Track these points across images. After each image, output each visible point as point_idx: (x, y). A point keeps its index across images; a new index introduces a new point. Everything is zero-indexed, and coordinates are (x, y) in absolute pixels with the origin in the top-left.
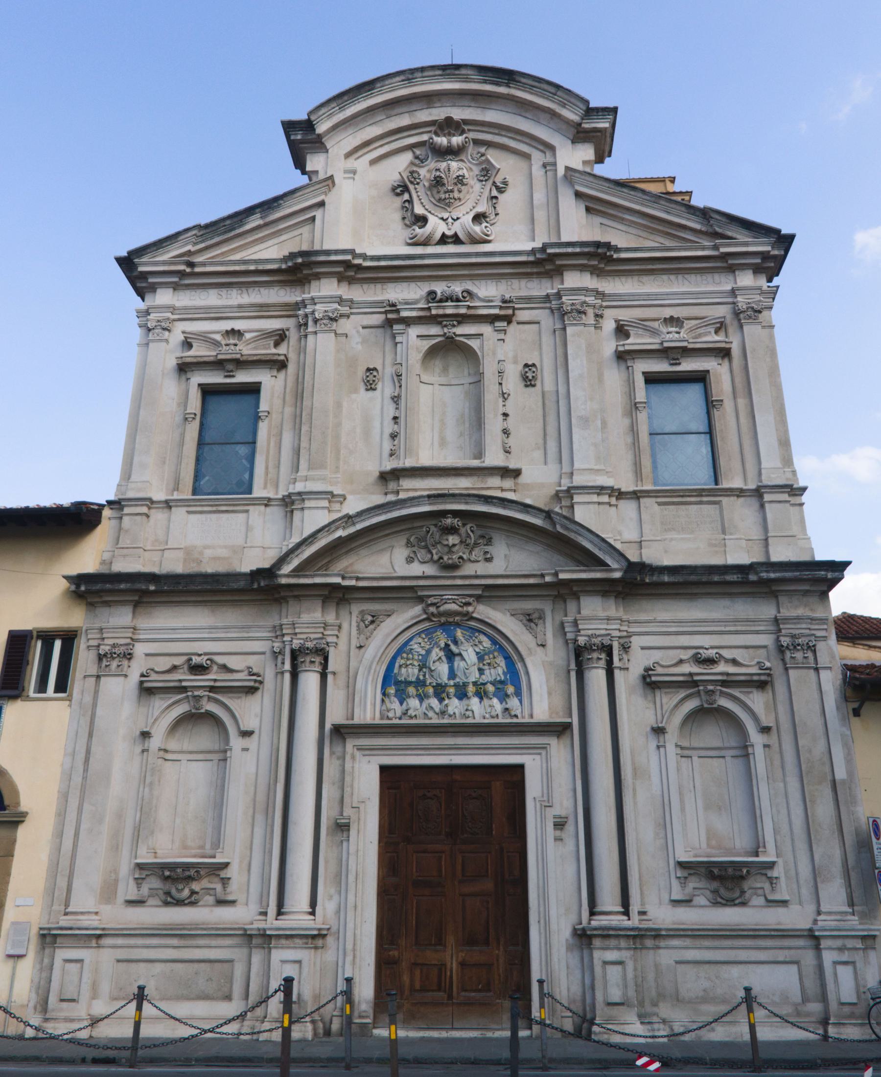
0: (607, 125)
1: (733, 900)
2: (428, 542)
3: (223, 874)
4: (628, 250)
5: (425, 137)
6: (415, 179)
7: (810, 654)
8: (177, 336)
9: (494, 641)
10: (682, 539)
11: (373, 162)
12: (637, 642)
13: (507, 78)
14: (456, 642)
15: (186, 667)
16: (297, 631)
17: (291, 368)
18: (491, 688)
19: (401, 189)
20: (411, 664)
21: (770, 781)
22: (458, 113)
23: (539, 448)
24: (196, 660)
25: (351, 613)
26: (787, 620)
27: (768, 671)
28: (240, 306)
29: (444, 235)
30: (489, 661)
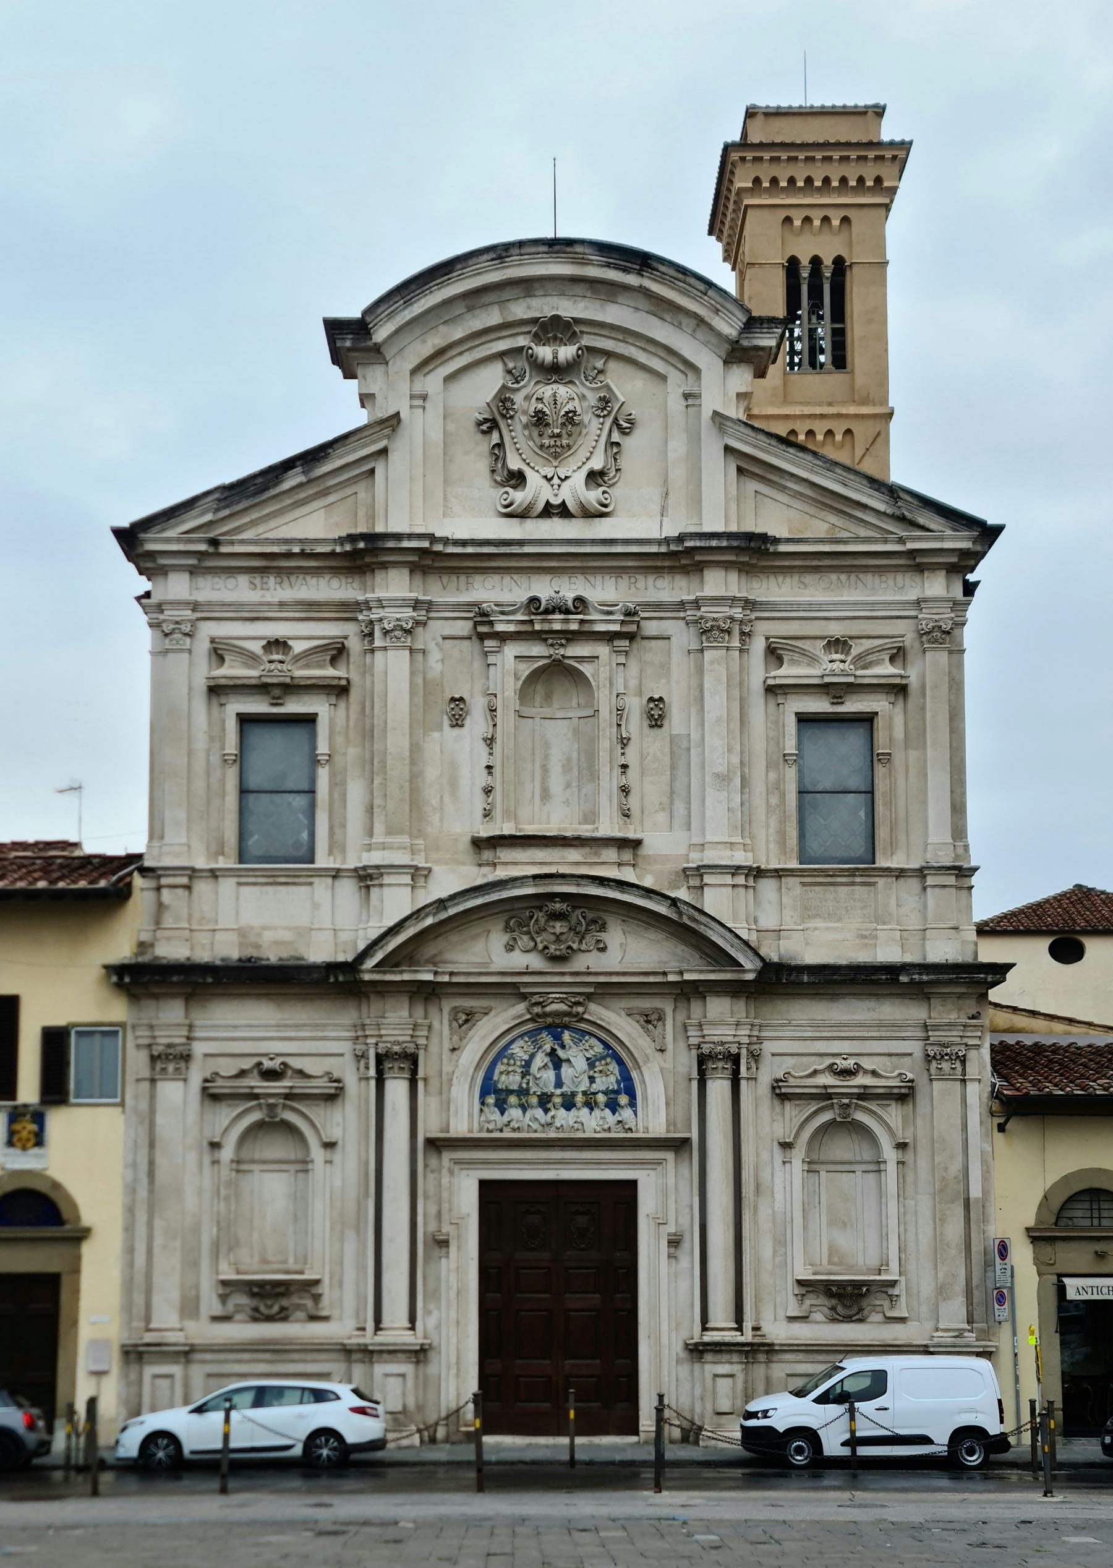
0: (773, 343)
1: (851, 1317)
2: (531, 927)
3: (314, 1290)
4: (789, 541)
5: (522, 341)
6: (508, 410)
7: (958, 1065)
8: (202, 646)
9: (607, 1046)
10: (827, 929)
11: (449, 379)
12: (769, 1047)
13: (639, 262)
14: (563, 1047)
15: (255, 1072)
16: (383, 1032)
17: (354, 694)
18: (601, 1098)
19: (488, 426)
20: (513, 1071)
21: (901, 1199)
22: (568, 308)
23: (663, 810)
24: (267, 1064)
25: (441, 1010)
26: (937, 1027)
27: (910, 1084)
28: (282, 604)
29: (548, 503)
30: (601, 1068)
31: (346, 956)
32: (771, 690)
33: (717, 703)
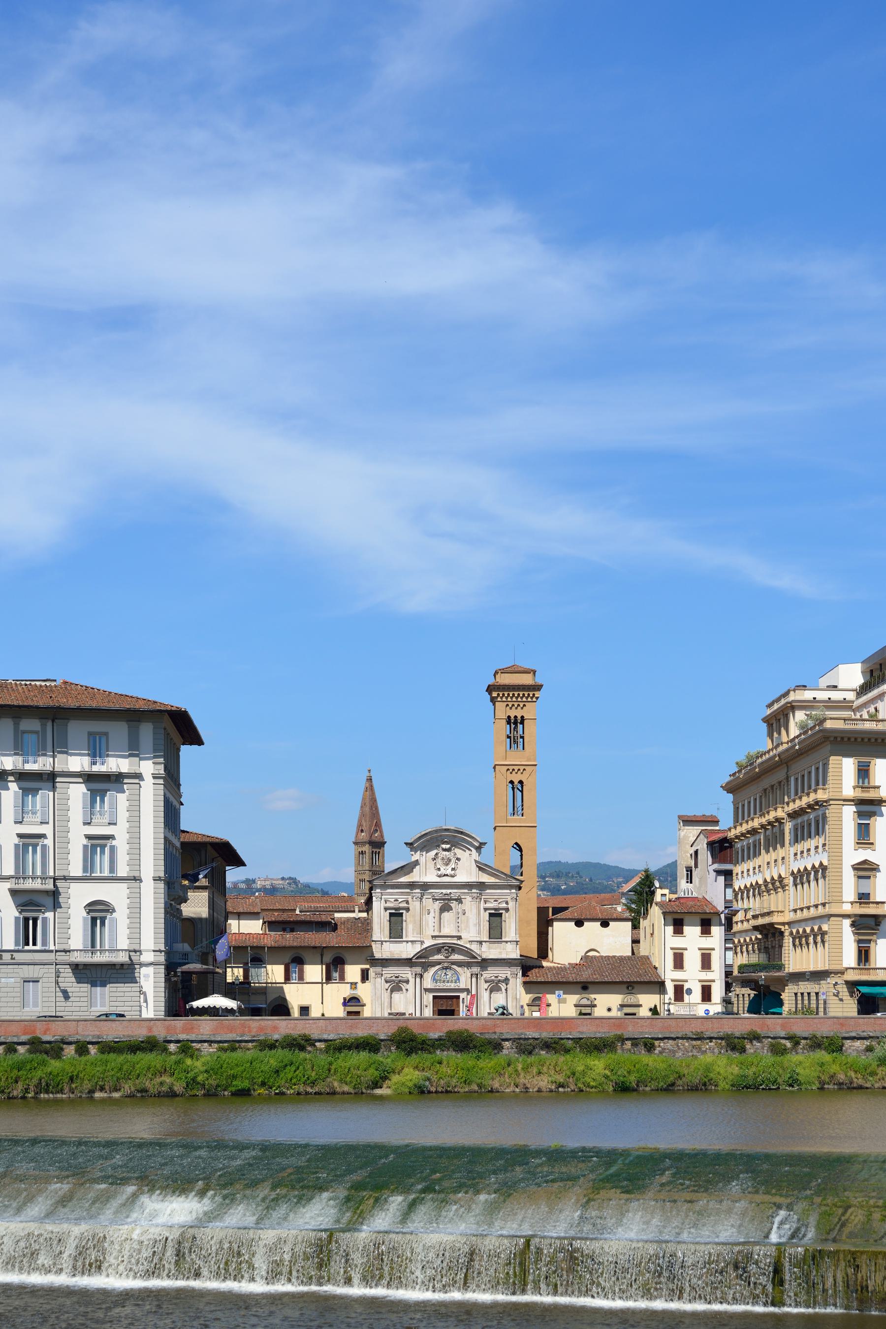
31: (410, 957)
32: (486, 909)
33: (474, 911)
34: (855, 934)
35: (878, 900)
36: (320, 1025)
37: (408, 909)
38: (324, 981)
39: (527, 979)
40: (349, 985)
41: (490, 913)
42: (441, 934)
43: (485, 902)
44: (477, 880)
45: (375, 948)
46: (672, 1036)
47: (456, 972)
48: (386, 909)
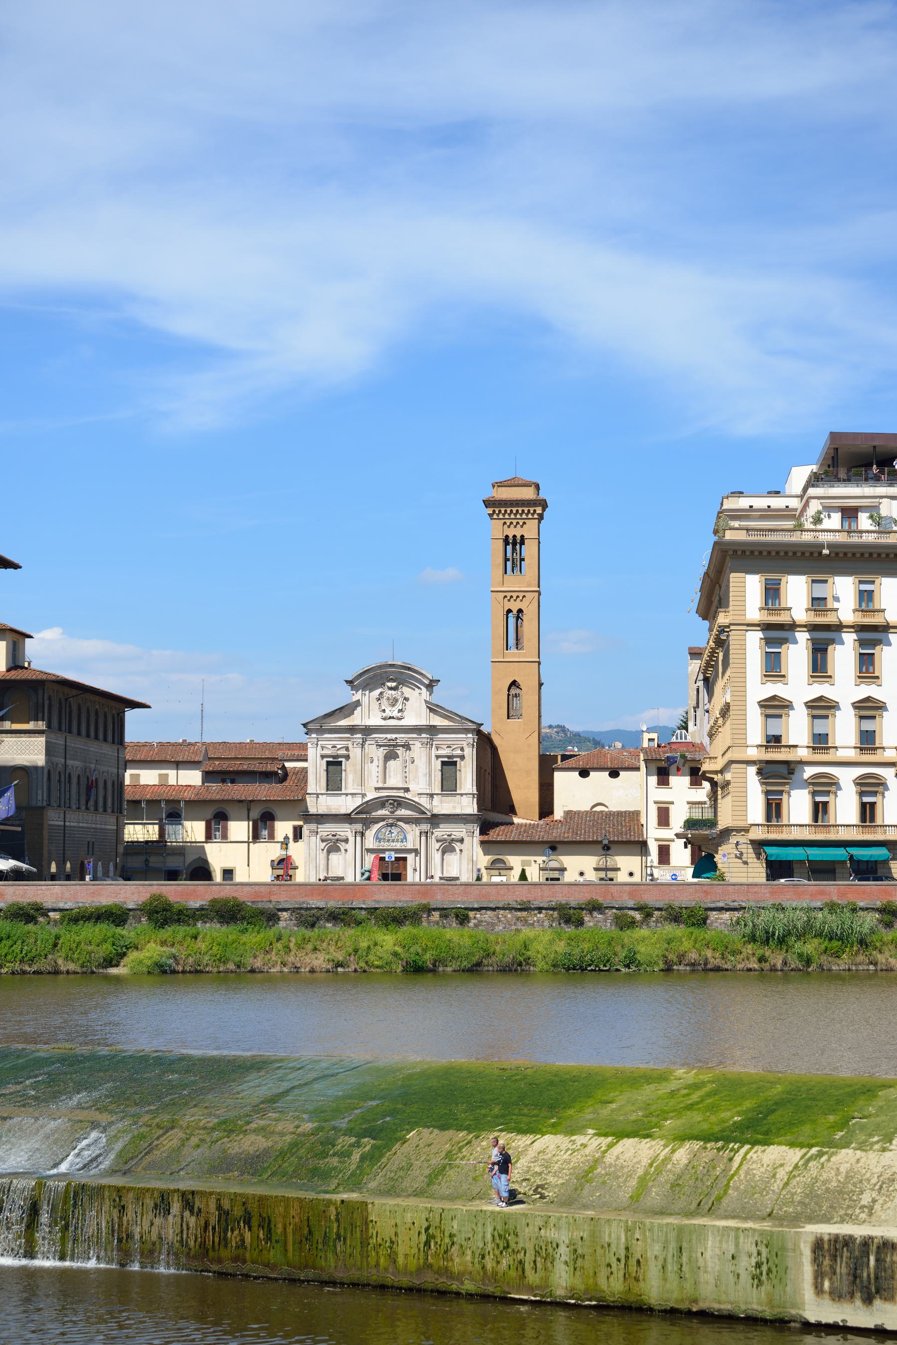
19: (378, 699)
24: (333, 833)
31: (349, 812)
32: (437, 757)
33: (424, 759)
34: (762, 784)
35: (791, 743)
36: (55, 891)
37: (347, 757)
38: (251, 840)
39: (486, 838)
40: (280, 844)
41: (442, 762)
42: (386, 786)
43: (437, 748)
44: (428, 724)
45: (310, 800)
46: (492, 905)
47: (403, 830)
48: (323, 757)
